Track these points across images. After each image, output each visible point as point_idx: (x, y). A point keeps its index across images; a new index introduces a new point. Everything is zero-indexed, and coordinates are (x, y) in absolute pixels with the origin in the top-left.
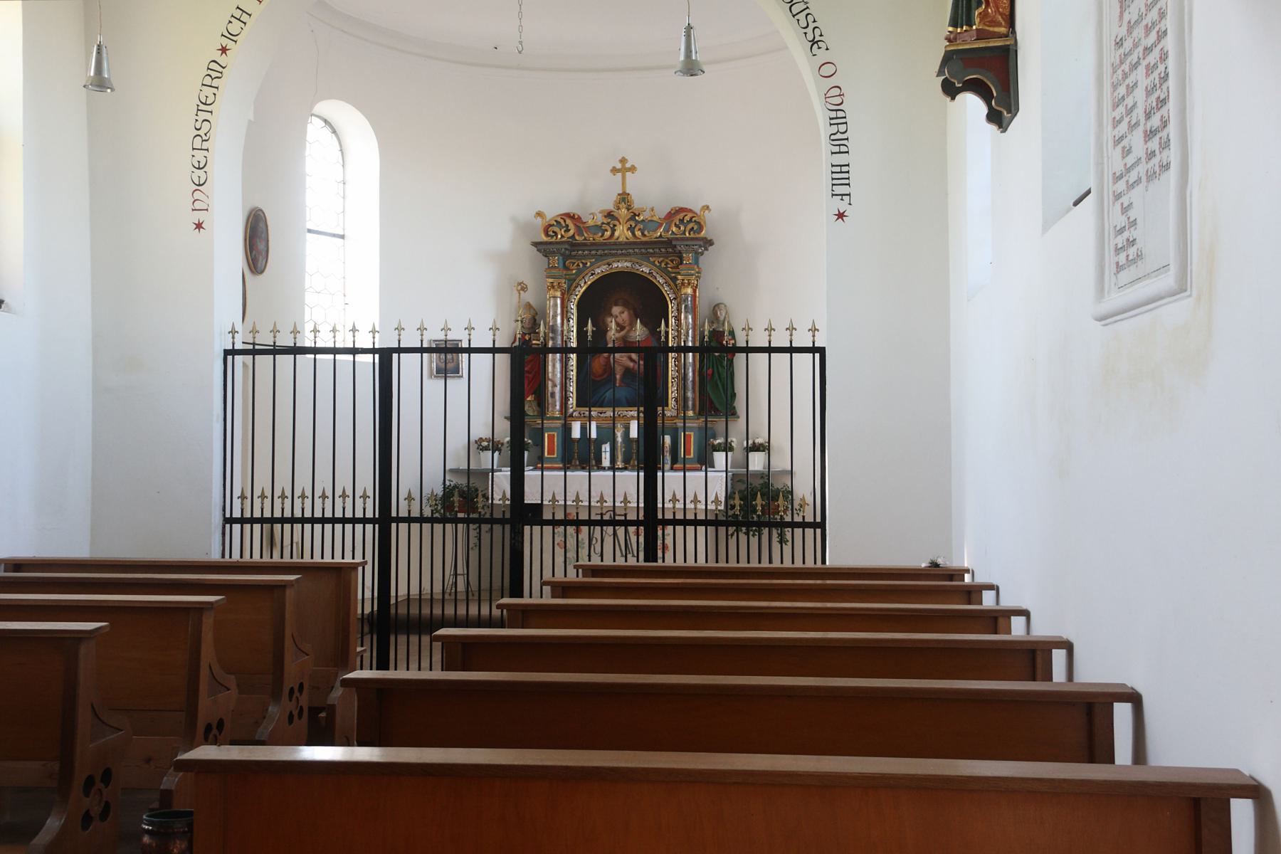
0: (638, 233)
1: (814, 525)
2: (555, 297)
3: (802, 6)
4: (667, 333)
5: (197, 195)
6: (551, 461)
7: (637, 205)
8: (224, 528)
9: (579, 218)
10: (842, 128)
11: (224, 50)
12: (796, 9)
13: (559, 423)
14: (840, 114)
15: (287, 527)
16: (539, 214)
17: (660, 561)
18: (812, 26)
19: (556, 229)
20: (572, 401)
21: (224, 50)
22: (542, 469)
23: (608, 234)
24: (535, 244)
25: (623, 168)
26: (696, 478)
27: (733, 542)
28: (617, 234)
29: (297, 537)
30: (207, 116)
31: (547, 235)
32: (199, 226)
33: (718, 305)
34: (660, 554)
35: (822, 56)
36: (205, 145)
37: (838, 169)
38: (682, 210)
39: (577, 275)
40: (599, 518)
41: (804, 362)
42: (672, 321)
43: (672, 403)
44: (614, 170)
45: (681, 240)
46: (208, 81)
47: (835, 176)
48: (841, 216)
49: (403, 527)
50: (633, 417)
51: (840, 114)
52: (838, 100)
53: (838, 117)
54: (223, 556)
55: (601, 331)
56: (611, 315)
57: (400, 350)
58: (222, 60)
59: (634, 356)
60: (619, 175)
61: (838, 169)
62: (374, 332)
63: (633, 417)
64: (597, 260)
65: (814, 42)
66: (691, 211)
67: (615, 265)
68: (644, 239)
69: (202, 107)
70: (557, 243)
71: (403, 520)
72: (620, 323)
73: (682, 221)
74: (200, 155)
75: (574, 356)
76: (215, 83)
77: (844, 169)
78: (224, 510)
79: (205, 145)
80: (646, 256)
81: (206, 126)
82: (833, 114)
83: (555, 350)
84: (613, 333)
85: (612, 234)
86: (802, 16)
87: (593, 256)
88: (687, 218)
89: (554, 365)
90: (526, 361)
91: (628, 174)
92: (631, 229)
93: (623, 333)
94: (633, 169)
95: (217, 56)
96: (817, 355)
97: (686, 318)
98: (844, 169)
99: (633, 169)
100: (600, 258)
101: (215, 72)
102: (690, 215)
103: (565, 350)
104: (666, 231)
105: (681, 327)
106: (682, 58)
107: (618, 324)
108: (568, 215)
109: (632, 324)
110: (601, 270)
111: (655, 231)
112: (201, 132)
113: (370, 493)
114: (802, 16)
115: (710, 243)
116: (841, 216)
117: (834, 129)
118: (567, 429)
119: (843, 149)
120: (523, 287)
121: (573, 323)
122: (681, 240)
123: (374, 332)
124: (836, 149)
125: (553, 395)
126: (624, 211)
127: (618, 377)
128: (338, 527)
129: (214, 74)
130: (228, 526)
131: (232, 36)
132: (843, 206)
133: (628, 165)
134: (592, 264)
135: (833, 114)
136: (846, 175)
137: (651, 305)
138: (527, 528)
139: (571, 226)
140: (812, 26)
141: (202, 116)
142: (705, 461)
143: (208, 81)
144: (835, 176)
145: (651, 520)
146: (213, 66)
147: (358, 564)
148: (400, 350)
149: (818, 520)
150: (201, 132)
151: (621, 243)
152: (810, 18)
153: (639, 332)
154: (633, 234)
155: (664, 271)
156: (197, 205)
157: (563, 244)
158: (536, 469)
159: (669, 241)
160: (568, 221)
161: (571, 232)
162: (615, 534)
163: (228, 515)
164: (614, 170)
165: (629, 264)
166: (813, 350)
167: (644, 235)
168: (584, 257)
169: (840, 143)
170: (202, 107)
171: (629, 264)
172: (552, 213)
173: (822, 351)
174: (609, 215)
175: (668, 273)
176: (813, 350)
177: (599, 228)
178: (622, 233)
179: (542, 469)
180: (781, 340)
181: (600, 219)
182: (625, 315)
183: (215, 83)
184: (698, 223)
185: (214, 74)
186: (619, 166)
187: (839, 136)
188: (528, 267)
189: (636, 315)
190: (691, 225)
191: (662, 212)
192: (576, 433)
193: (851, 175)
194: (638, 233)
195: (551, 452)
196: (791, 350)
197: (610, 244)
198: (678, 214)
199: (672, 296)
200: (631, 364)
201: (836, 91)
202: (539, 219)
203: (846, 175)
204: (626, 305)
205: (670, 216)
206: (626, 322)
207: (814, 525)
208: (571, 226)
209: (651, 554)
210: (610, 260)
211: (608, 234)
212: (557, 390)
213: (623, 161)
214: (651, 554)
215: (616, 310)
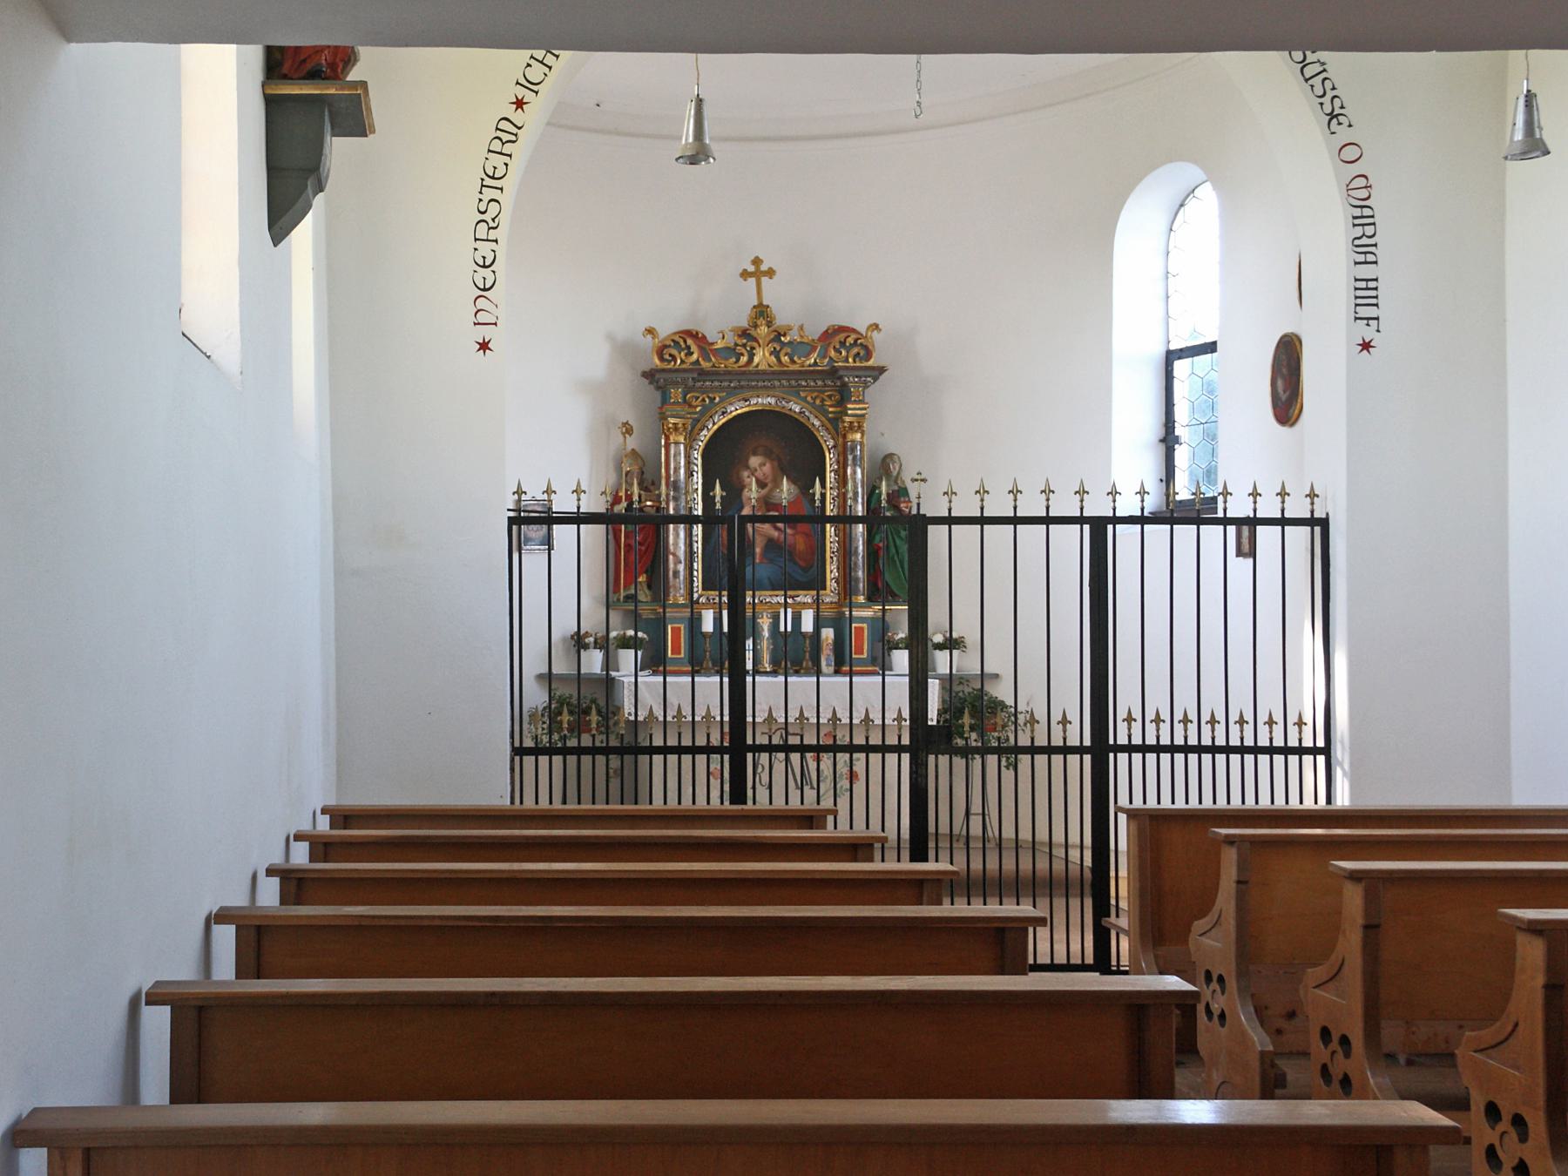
0: (785, 359)
1: (1314, 751)
2: (677, 443)
3: (1318, 68)
4: (823, 496)
5: (481, 303)
6: (862, 662)
7: (781, 320)
8: (512, 761)
9: (704, 337)
10: (1369, 230)
11: (520, 104)
12: (1309, 72)
13: (687, 613)
14: (1367, 212)
15: (875, 758)
16: (650, 331)
17: (750, 802)
18: (1330, 94)
19: (674, 352)
20: (698, 583)
21: (520, 104)
22: (851, 674)
23: (744, 359)
24: (645, 375)
25: (758, 272)
26: (867, 685)
27: (1008, 775)
28: (756, 360)
29: (572, 771)
30: (495, 194)
31: (662, 359)
32: (484, 346)
33: (891, 455)
34: (750, 793)
35: (1344, 135)
36: (493, 235)
37: (1363, 285)
38: (842, 329)
39: (702, 413)
40: (831, 742)
41: (1299, 537)
42: (830, 477)
43: (831, 584)
44: (745, 274)
45: (843, 367)
46: (496, 145)
47: (1360, 293)
48: (1366, 346)
49: (1123, 757)
50: (805, 605)
51: (1367, 212)
52: (1364, 193)
53: (1363, 216)
54: (512, 802)
55: (734, 492)
56: (748, 467)
57: (1116, 520)
58: (517, 117)
59: (780, 525)
60: (752, 280)
61: (1363, 285)
62: (578, 491)
63: (805, 605)
64: (730, 395)
65: (1332, 116)
66: (854, 331)
67: (754, 401)
68: (795, 367)
69: (488, 182)
70: (677, 371)
71: (1123, 749)
72: (762, 482)
73: (843, 344)
74: (485, 249)
75: (860, 528)
76: (507, 149)
77: (1371, 284)
78: (512, 737)
79: (493, 235)
80: (795, 392)
81: (494, 207)
82: (1358, 212)
83: (677, 519)
84: (752, 493)
85: (751, 360)
86: (1317, 81)
87: (721, 389)
88: (850, 340)
89: (676, 537)
90: (634, 531)
91: (764, 280)
92: (775, 353)
93: (764, 492)
94: (770, 273)
95: (509, 111)
96: (1317, 529)
97: (854, 472)
98: (1371, 284)
99: (770, 273)
100: (732, 392)
101: (506, 133)
102: (853, 336)
103: (689, 520)
104: (824, 355)
105: (843, 487)
106: (1519, 136)
107: (758, 481)
108: (689, 333)
109: (777, 484)
110: (737, 409)
111: (807, 356)
112: (487, 217)
113: (1073, 716)
114: (1317, 81)
115: (882, 370)
116: (1366, 346)
117: (1358, 231)
118: (694, 622)
119: (1370, 258)
120: (628, 429)
121: (698, 478)
122: (843, 367)
123: (578, 491)
124: (1361, 258)
125: (676, 573)
126: (763, 330)
127: (758, 550)
128: (1166, 757)
129: (505, 137)
130: (517, 758)
131: (531, 86)
132: (1369, 333)
133: (764, 268)
134: (722, 400)
135: (1358, 212)
136: (1373, 293)
137: (802, 457)
138: (931, 758)
139: (694, 348)
140: (1330, 94)
141: (489, 194)
142: (882, 665)
143: (496, 145)
144: (1360, 293)
145: (737, 745)
146: (504, 125)
147: (829, 811)
148: (1116, 520)
149: (1321, 743)
150: (487, 217)
151: (764, 372)
152: (1328, 84)
153: (786, 491)
154: (779, 360)
155: (821, 410)
156: (482, 317)
157: (676, 372)
158: (655, 673)
159: (833, 372)
160: (690, 342)
161: (695, 356)
162: (787, 759)
163: (517, 744)
164: (745, 274)
165: (772, 401)
166: (1311, 522)
167: (793, 362)
168: (713, 389)
169: (1364, 250)
170: (488, 182)
171: (772, 401)
172: (666, 329)
173: (1324, 523)
174: (744, 333)
175: (825, 413)
176: (1311, 522)
177: (731, 351)
178: (762, 357)
179: (851, 674)
180: (1031, 506)
181: (731, 339)
182: (767, 468)
183: (507, 149)
184: (865, 347)
185: (505, 137)
186: (751, 269)
187: (1365, 241)
188: (629, 402)
189: (783, 469)
190: (855, 350)
191: (814, 332)
192: (708, 625)
193: (1380, 293)
194: (785, 359)
195: (676, 650)
196: (982, 521)
197: (750, 373)
198: (837, 335)
199: (831, 443)
200: (776, 534)
201: (1362, 182)
202: (649, 337)
203: (1373, 293)
204: (768, 454)
205: (828, 335)
206: (764, 475)
207: (1314, 751)
208: (694, 348)
209: (738, 794)
210: (747, 394)
211: (744, 359)
212: (681, 567)
213: (757, 261)
214: (738, 794)
215: (754, 461)
